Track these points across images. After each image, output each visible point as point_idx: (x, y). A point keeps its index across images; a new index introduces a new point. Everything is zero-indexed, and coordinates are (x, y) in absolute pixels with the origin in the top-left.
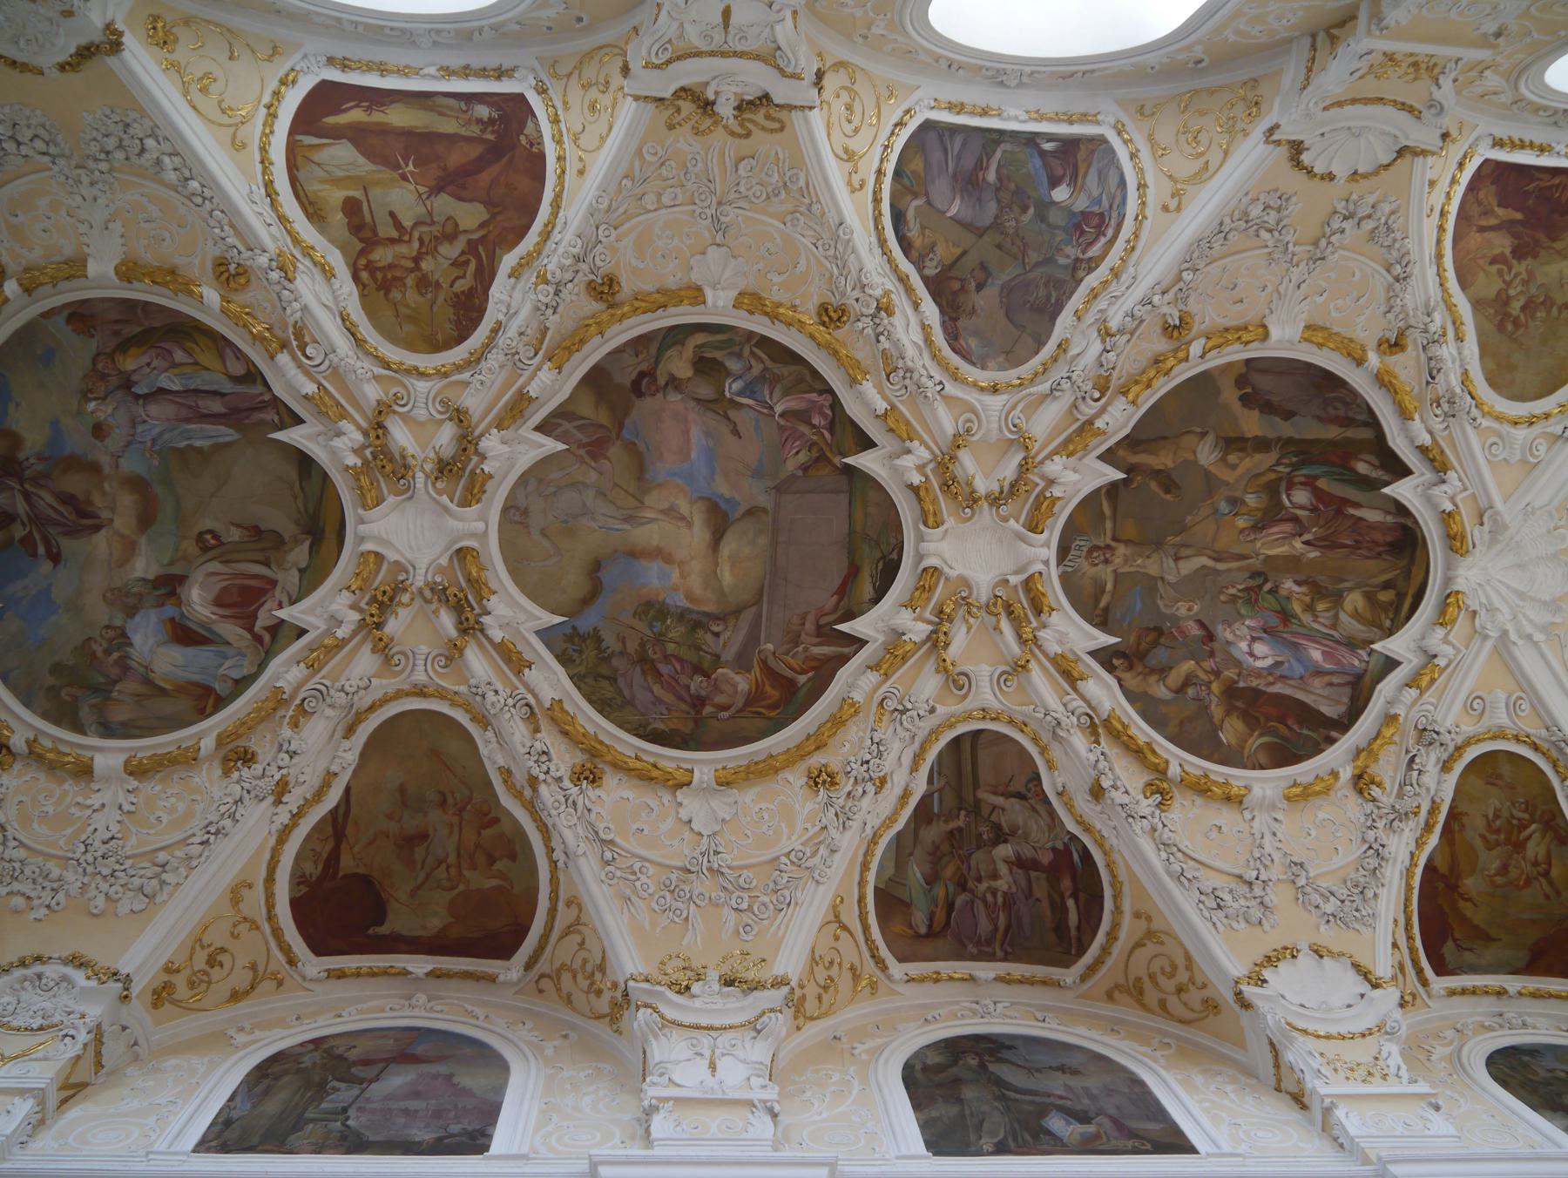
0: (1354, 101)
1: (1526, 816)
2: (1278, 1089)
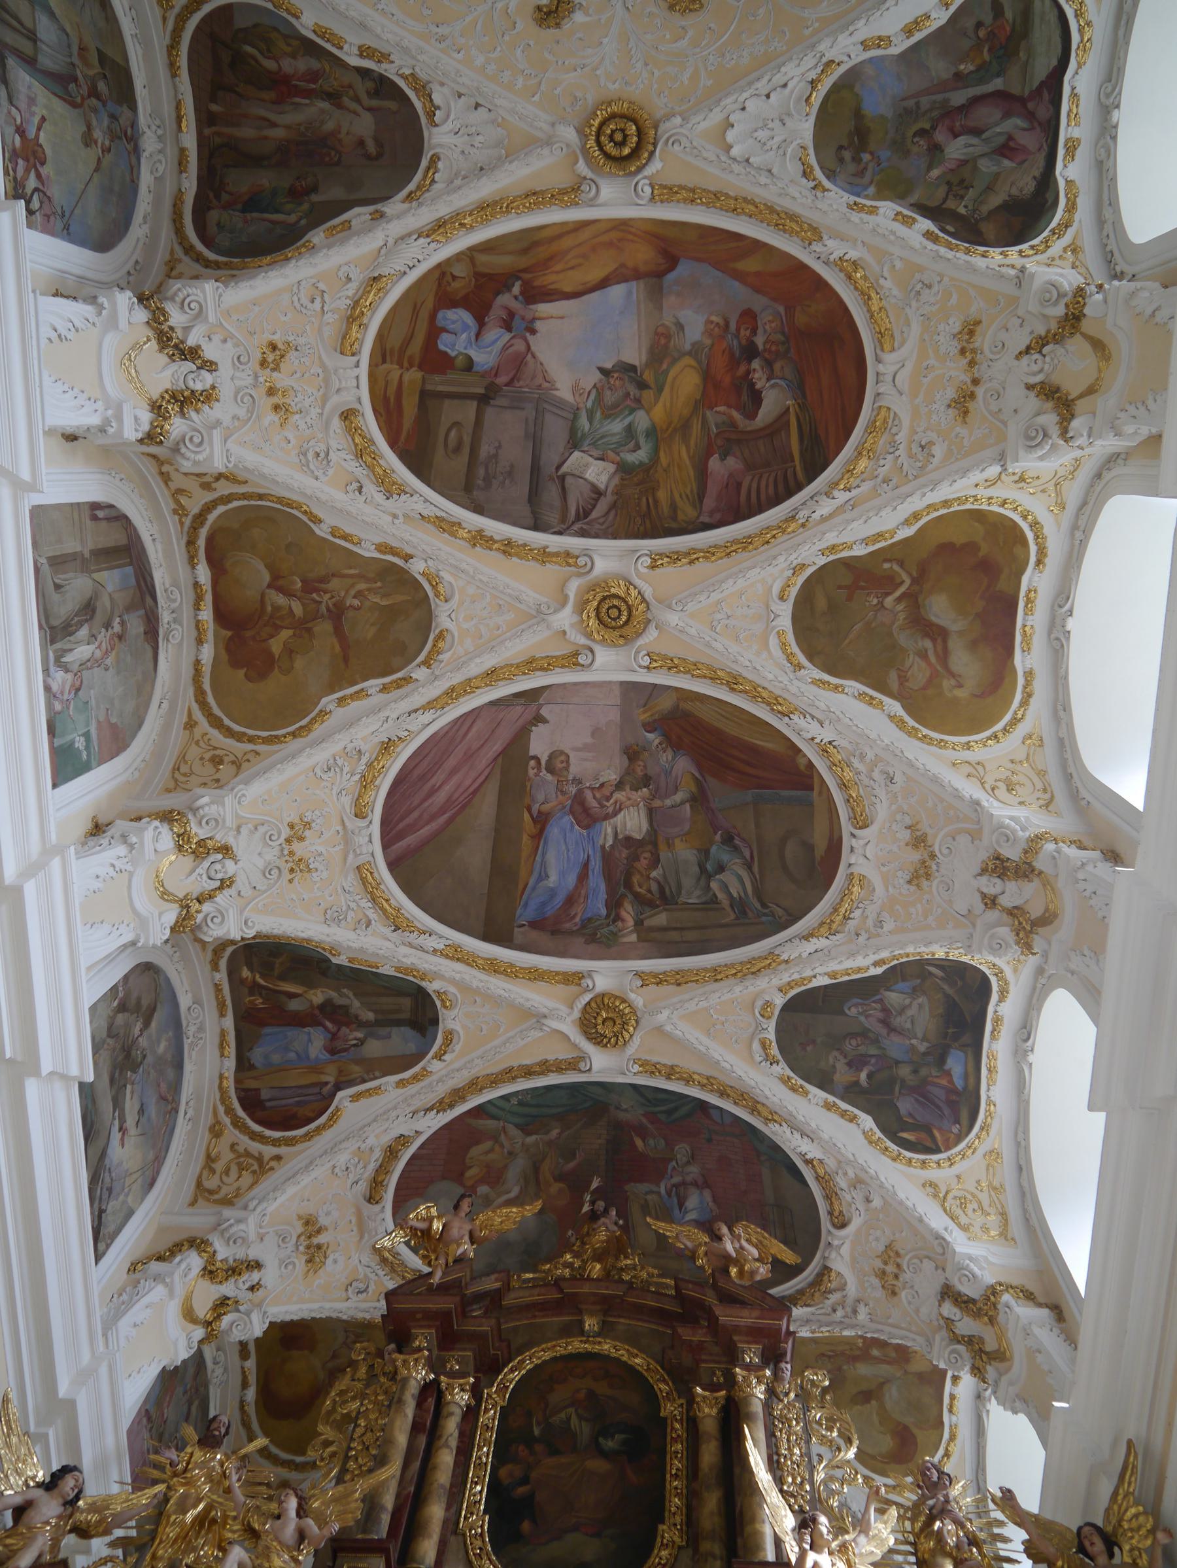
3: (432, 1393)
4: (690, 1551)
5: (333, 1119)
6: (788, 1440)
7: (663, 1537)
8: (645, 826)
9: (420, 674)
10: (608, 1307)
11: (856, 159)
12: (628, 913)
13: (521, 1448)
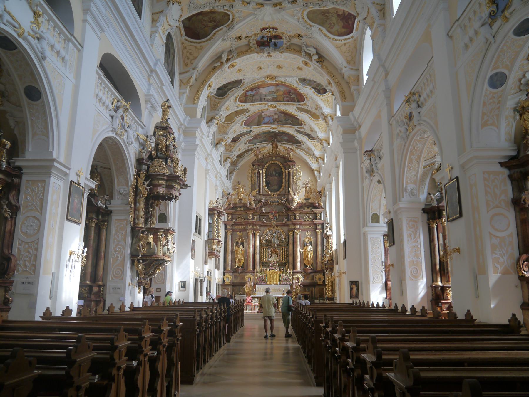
0: (368, 12)
1: (217, 22)
2: (153, 14)
3: (259, 172)
5: (240, 140)
8: (278, 117)
9: (247, 114)
10: (276, 157)
11: (304, 82)
12: (276, 122)
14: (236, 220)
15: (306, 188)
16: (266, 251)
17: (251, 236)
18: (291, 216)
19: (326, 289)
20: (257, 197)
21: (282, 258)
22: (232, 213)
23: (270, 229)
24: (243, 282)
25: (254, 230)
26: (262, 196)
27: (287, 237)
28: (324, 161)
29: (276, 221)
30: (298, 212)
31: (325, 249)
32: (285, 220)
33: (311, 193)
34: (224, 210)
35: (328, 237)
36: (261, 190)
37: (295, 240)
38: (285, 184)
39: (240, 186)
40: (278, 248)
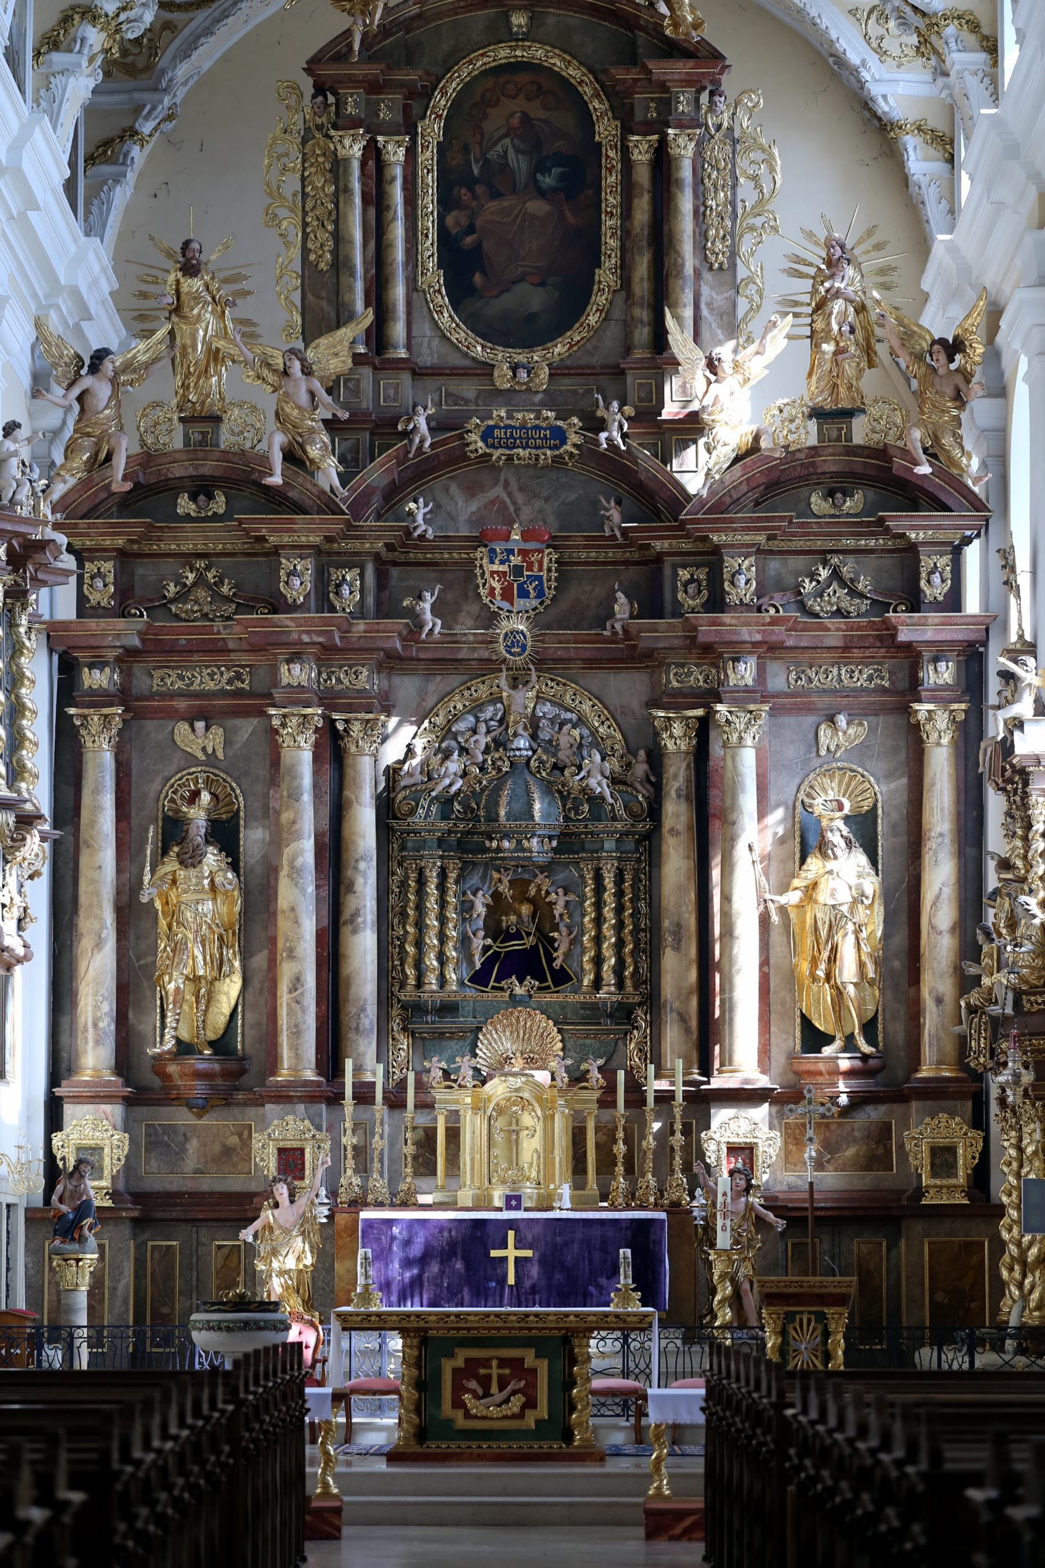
3: (373, 154)
4: (623, 294)
6: (716, 188)
7: (600, 282)
13: (463, 191)
14: (159, 606)
15: (821, 306)
16: (443, 904)
17: (307, 756)
18: (684, 574)
19: (1000, 1246)
20: (356, 392)
21: (598, 961)
22: (120, 542)
23: (483, 692)
24: (234, 1184)
25: (329, 700)
26: (406, 378)
27: (641, 768)
28: (992, 47)
29: (536, 620)
30: (748, 538)
31: (992, 881)
32: (622, 607)
33: (868, 352)
34: (57, 527)
35: (1024, 774)
36: (398, 330)
37: (713, 793)
38: (625, 269)
39: (194, 285)
40: (561, 876)
